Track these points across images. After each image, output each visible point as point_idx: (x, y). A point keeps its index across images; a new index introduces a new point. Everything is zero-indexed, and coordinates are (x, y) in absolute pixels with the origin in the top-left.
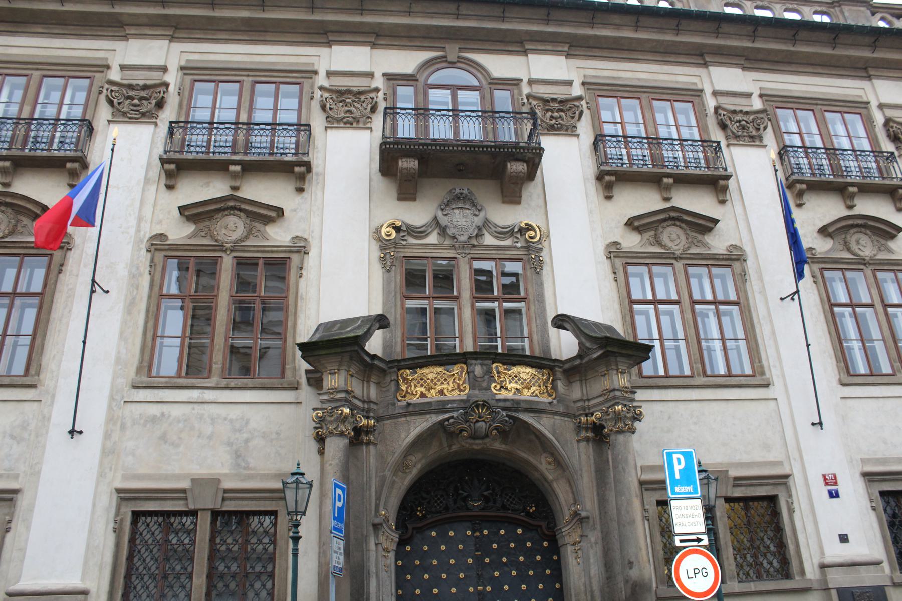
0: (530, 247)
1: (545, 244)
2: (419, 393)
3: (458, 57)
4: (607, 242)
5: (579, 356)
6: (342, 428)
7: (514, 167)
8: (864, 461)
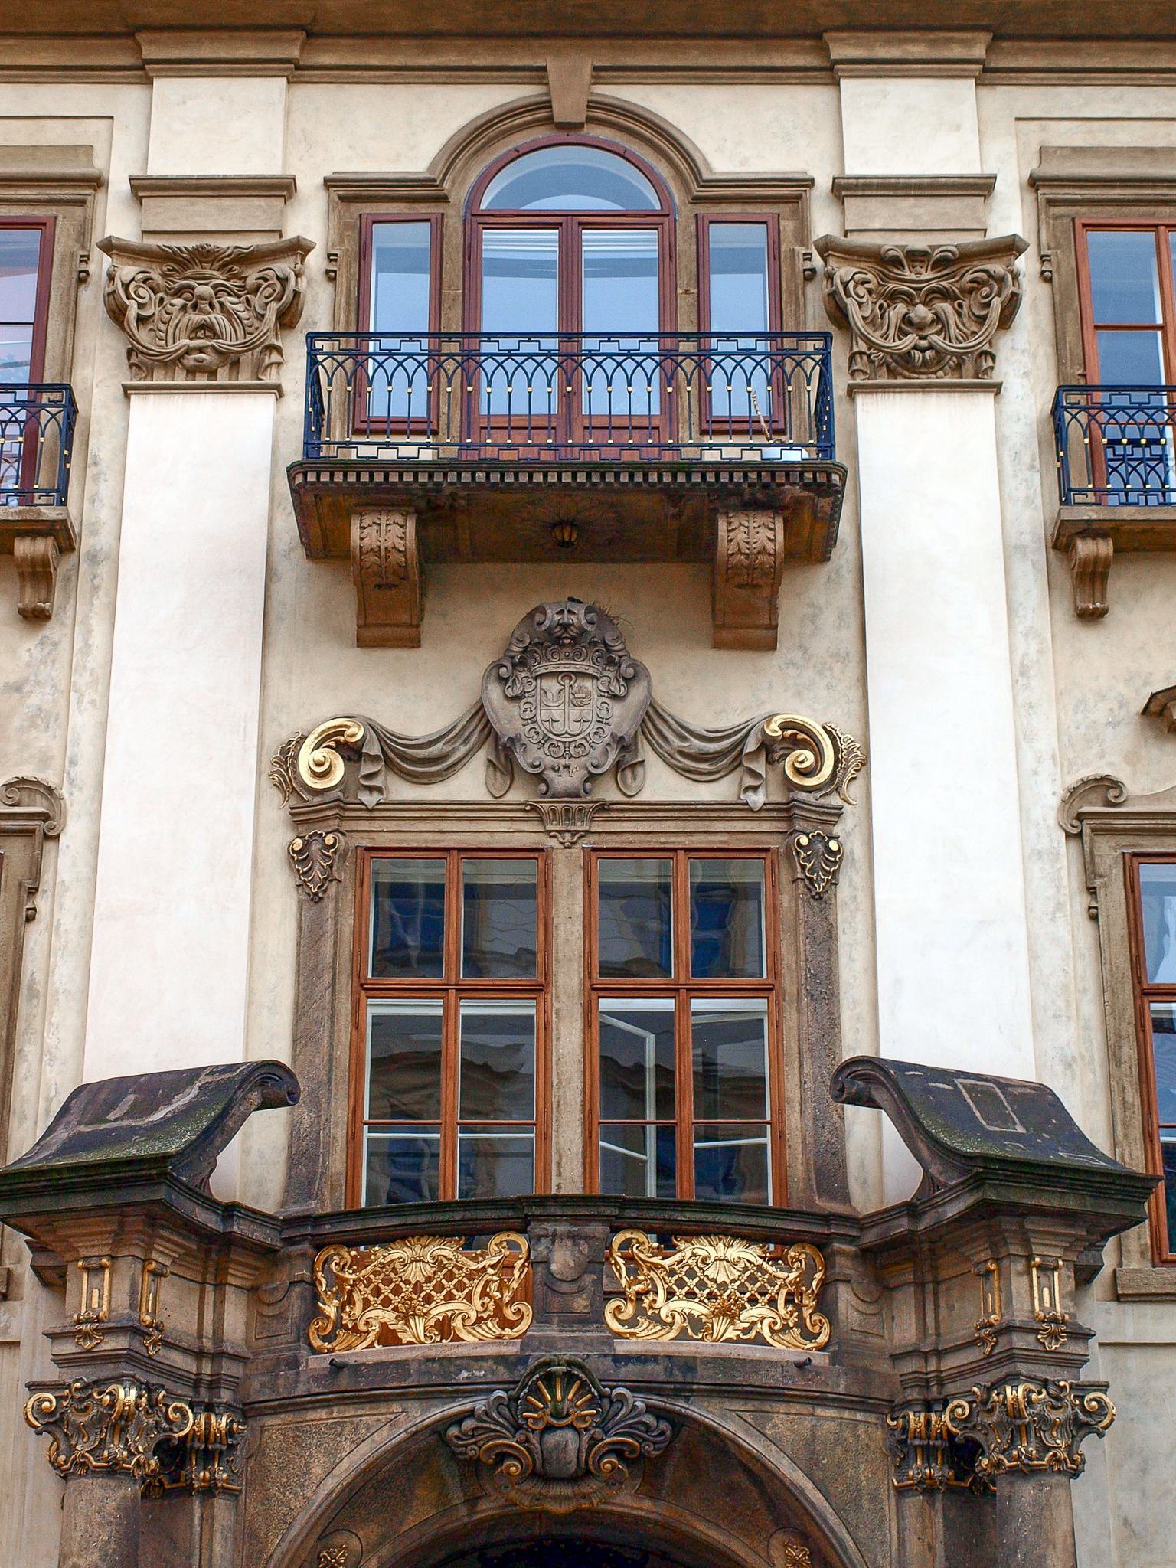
1: (854, 791)
2: (376, 1327)
3: (592, 105)
4: (1072, 780)
5: (911, 1209)
6: (116, 1449)
7: (741, 536)
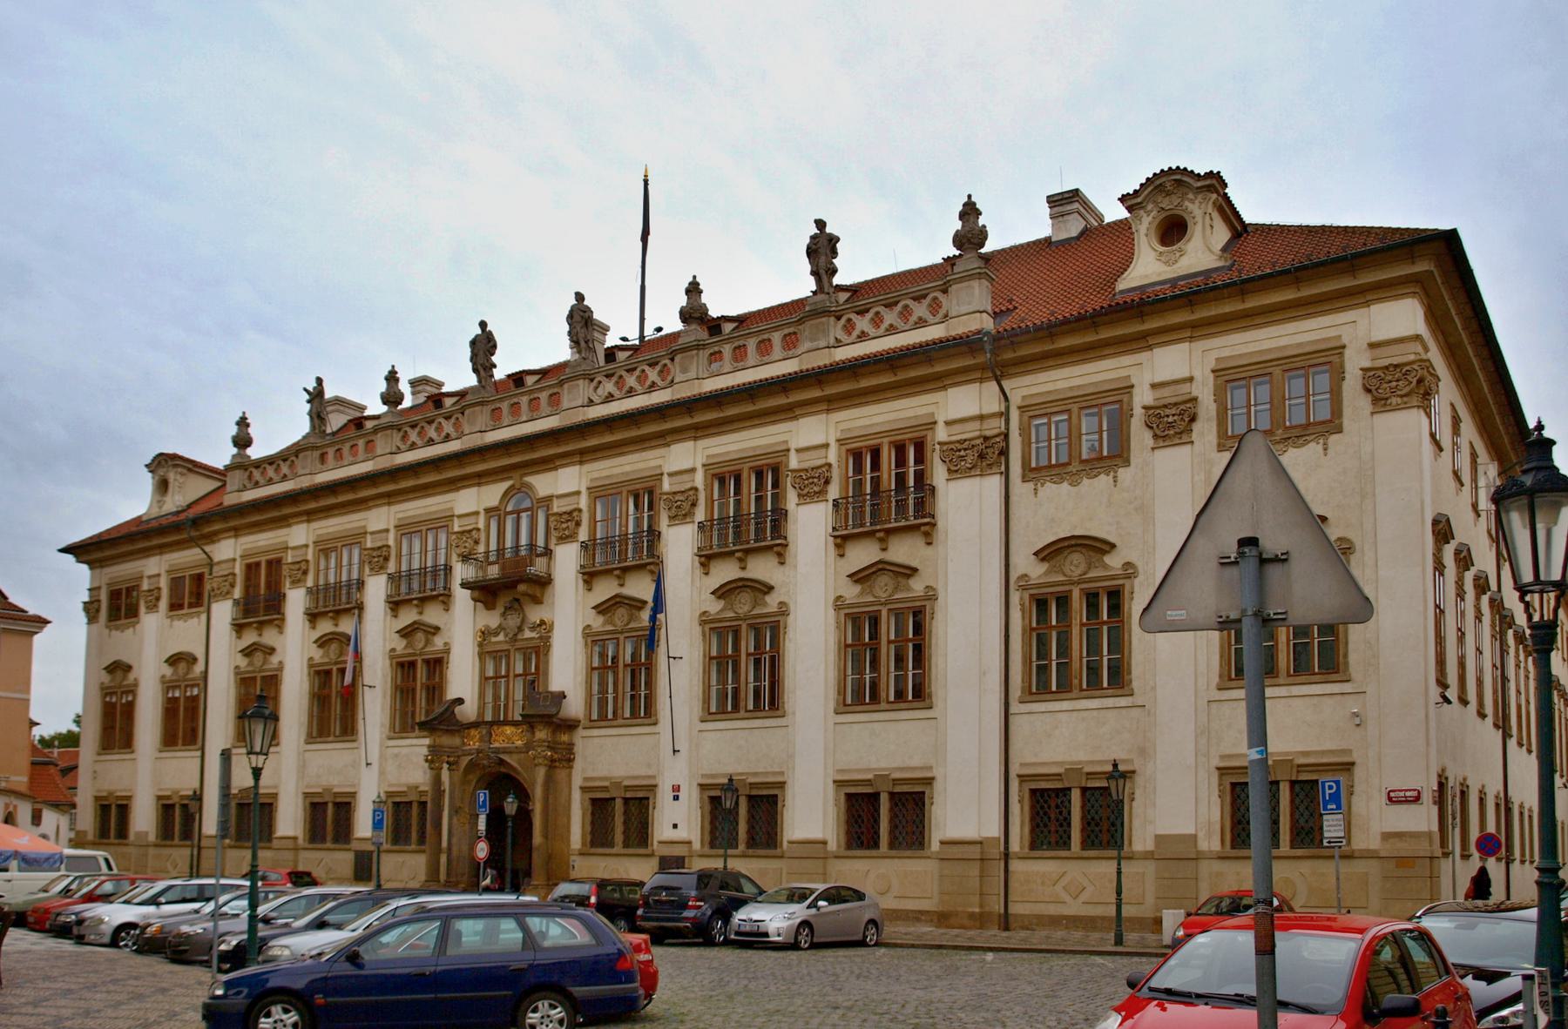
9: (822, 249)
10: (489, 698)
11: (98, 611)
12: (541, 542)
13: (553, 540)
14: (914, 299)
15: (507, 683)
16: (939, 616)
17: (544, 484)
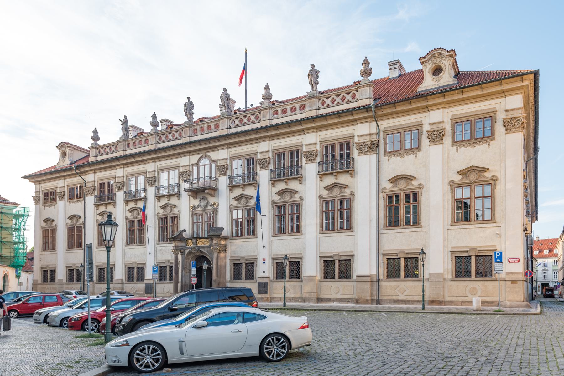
0: (215, 207)
8: (274, 255)
9: (314, 75)
10: (195, 230)
11: (39, 200)
12: (213, 175)
13: (218, 175)
14: (347, 93)
15: (202, 225)
16: (355, 201)
17: (214, 155)
